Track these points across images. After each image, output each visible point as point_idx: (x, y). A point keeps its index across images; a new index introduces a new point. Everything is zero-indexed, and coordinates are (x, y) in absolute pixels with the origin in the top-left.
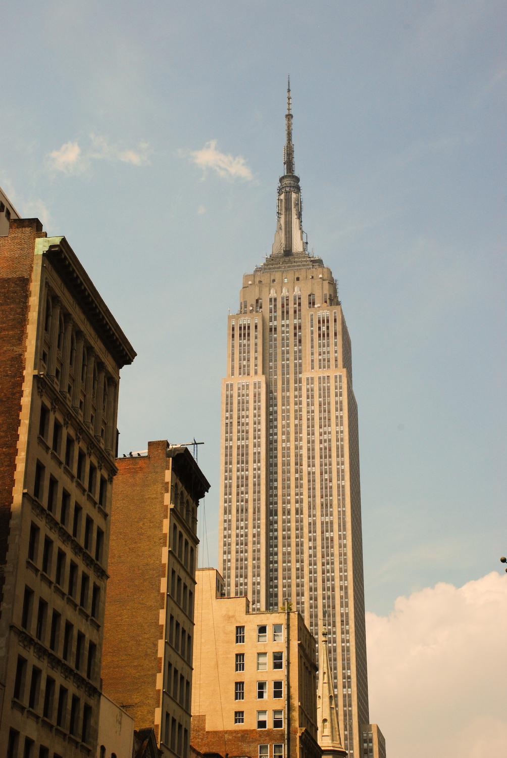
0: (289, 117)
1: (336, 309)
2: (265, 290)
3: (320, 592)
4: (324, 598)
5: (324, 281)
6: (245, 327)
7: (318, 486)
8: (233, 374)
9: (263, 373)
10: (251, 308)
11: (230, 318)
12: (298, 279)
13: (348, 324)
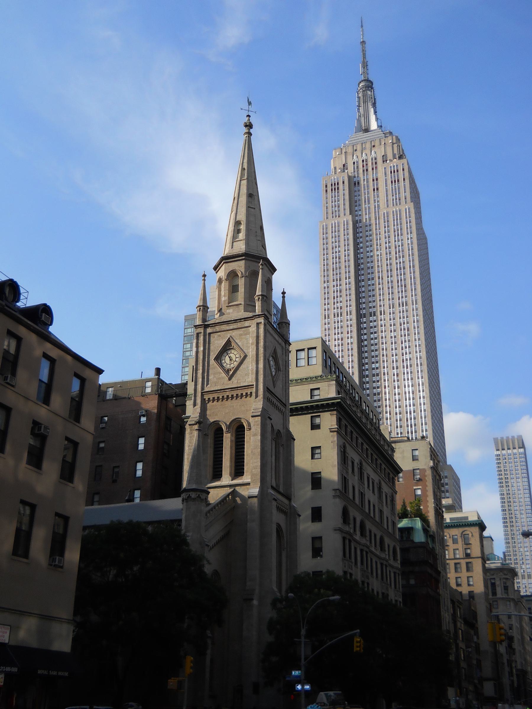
1: (404, 161)
2: (350, 157)
6: (335, 184)
9: (350, 214)
13: (413, 173)
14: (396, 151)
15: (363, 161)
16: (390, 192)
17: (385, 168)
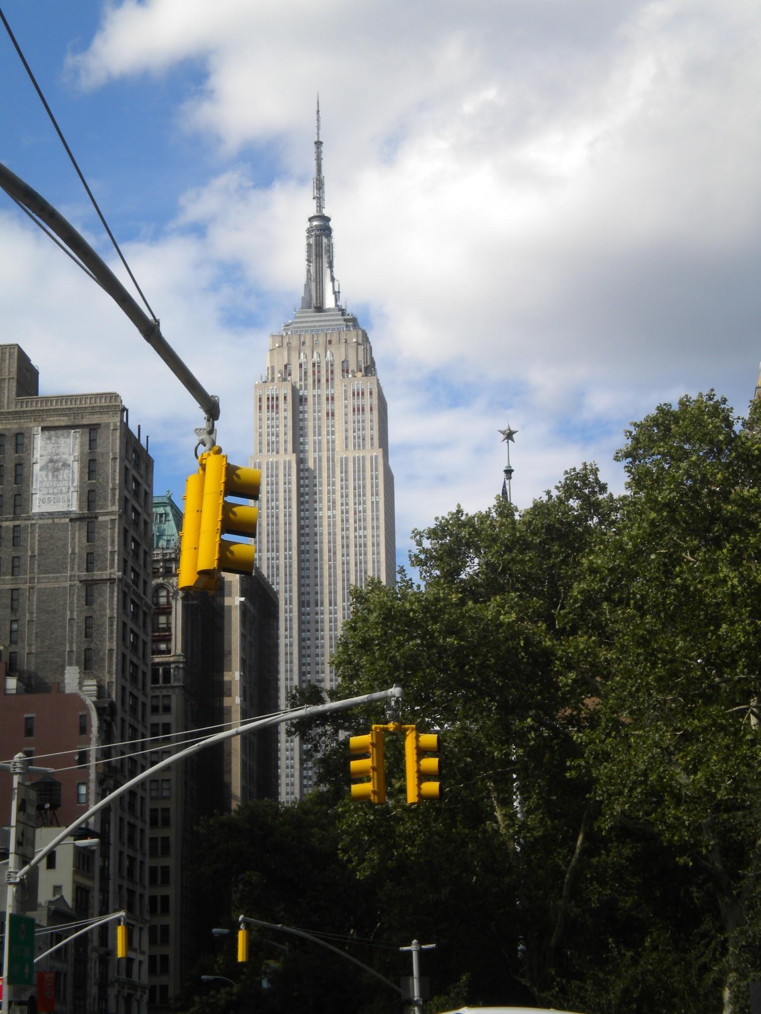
0: (319, 144)
1: (374, 379)
2: (294, 355)
5: (359, 346)
6: (273, 398)
8: (261, 451)
9: (293, 453)
10: (279, 375)
11: (256, 387)
12: (330, 342)
14: (361, 358)
15: (314, 365)
16: (351, 426)
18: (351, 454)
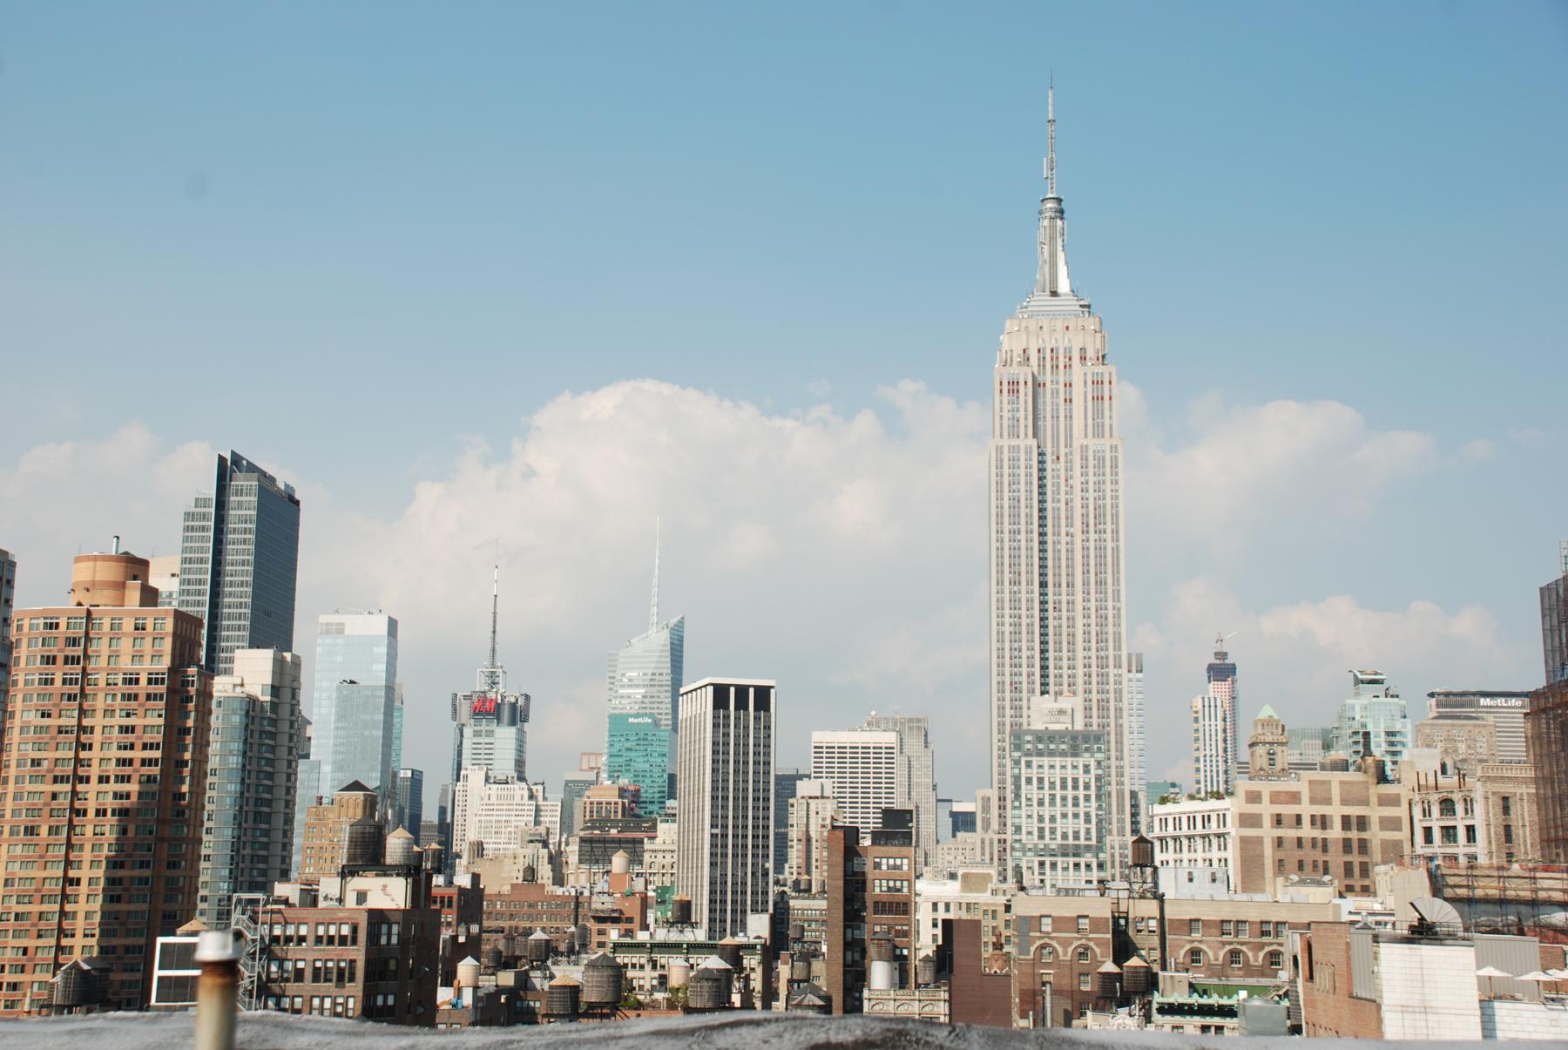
3: (1094, 669)
4: (1098, 676)
7: (1092, 563)
9: (1034, 437)
12: (1067, 328)
15: (1052, 350)
17: (1085, 374)
18: (1091, 442)
